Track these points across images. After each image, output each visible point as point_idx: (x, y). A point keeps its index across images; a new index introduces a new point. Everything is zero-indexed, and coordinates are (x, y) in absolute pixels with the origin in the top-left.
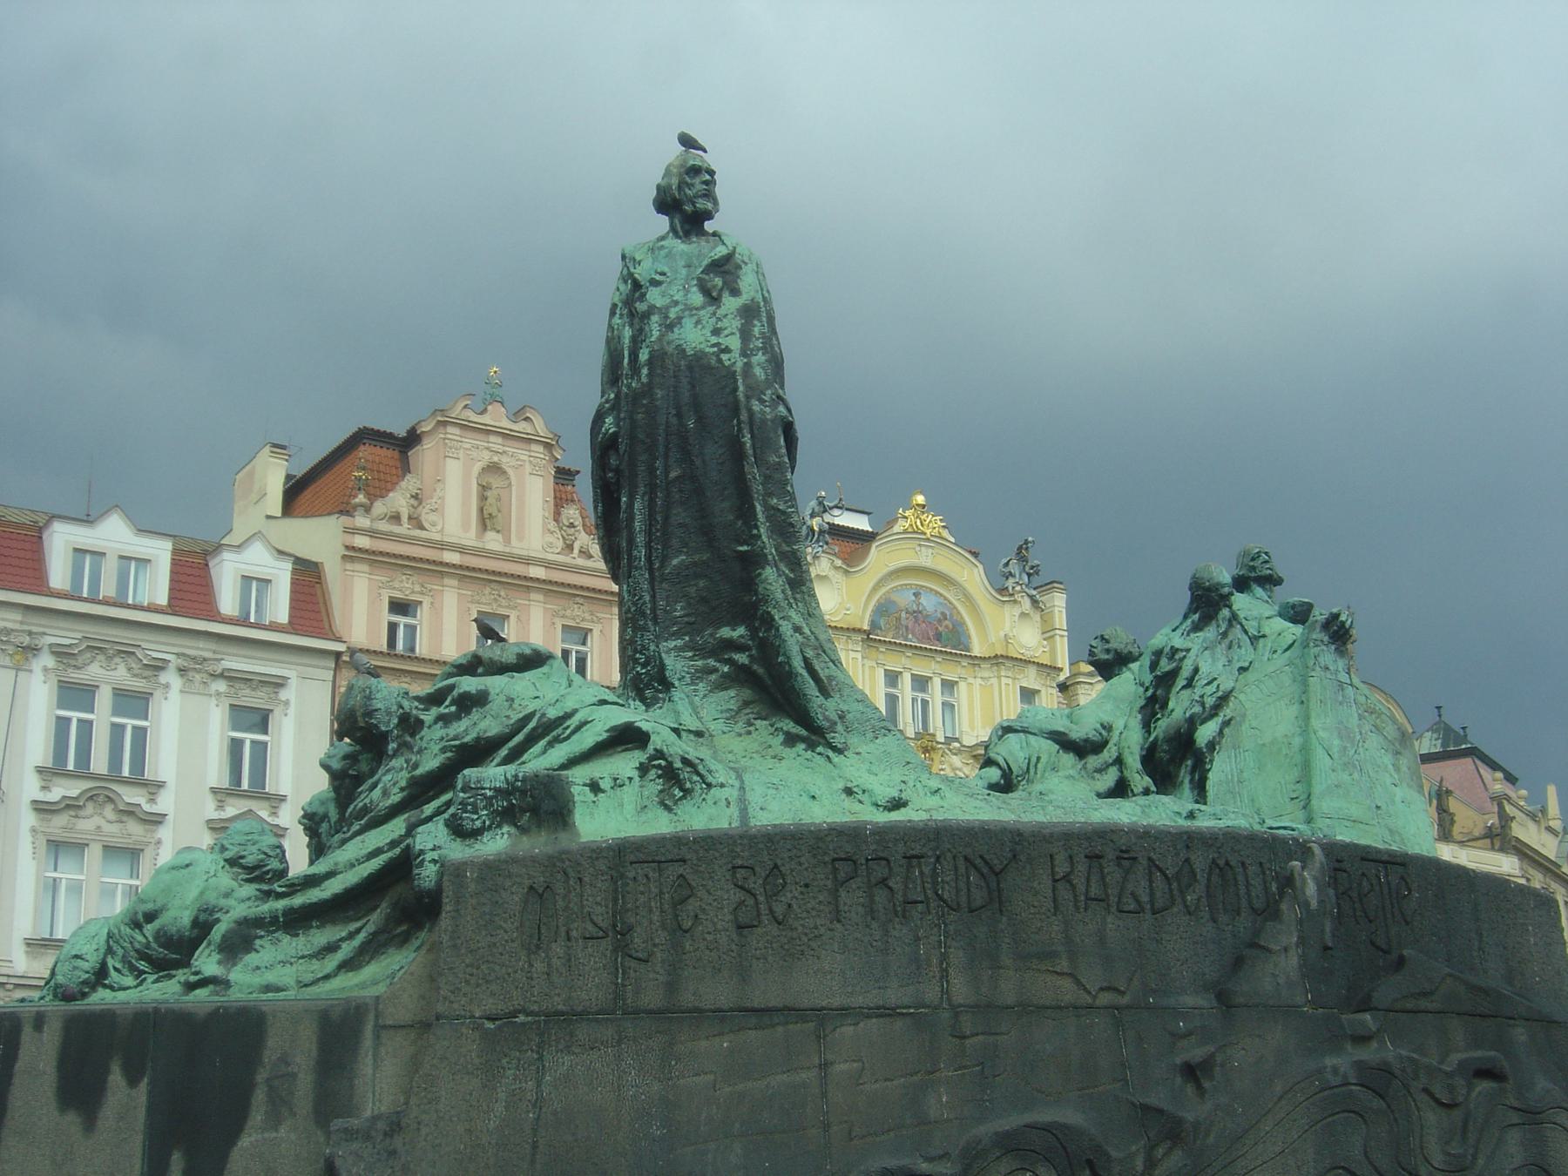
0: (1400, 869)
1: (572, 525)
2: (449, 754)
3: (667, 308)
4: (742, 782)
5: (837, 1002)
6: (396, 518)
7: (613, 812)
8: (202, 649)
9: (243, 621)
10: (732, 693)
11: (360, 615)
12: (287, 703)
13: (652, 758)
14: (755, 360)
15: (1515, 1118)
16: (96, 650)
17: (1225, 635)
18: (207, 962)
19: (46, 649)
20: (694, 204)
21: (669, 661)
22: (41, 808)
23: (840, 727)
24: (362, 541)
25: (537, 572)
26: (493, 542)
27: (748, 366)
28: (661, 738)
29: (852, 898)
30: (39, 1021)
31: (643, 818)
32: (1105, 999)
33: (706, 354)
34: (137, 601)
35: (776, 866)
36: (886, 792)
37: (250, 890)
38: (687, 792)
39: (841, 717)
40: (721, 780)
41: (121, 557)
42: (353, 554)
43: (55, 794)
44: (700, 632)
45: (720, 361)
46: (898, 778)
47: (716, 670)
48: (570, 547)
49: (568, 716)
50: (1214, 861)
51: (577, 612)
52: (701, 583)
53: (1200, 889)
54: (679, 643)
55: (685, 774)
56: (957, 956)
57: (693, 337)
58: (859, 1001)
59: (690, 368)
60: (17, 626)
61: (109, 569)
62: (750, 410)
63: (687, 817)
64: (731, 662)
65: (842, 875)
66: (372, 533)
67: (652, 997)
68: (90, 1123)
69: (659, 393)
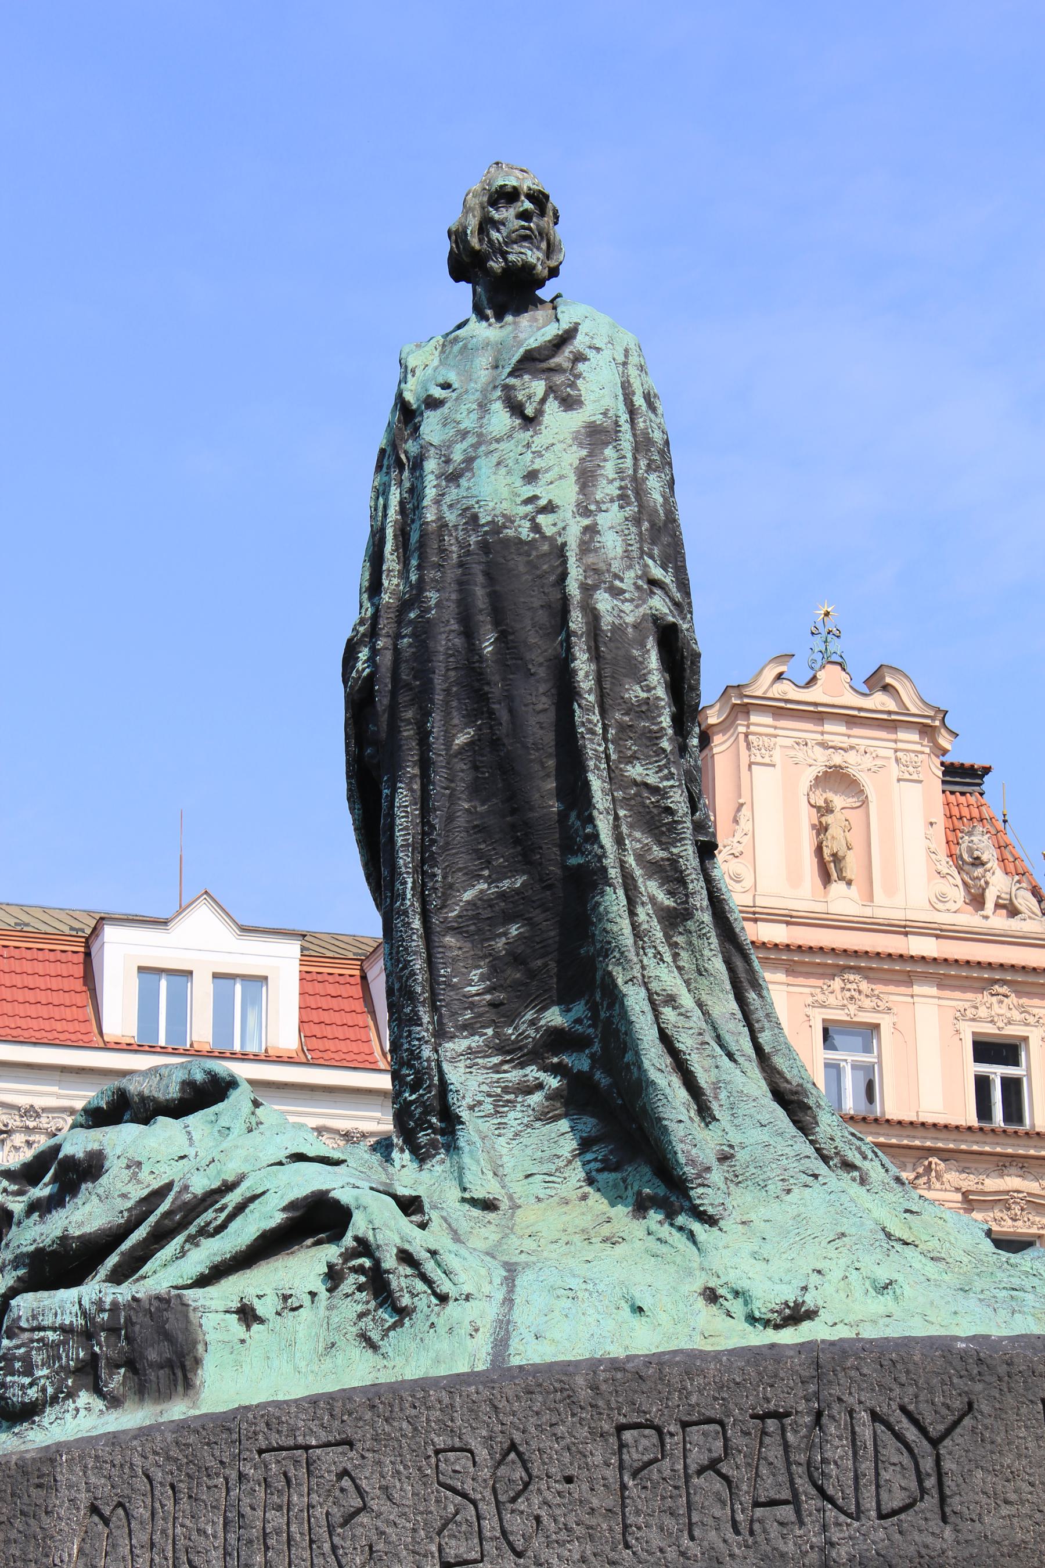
1: (978, 862)
2: (21, 1272)
3: (449, 445)
4: (511, 1290)
7: (271, 1351)
10: (564, 1125)
13: (349, 1255)
14: (604, 520)
20: (504, 254)
21: (455, 1075)
23: (716, 1176)
26: (842, 900)
28: (378, 1221)
31: (328, 1364)
33: (509, 520)
34: (252, 1048)
35: (513, 1447)
36: (771, 1292)
38: (403, 1313)
39: (724, 1158)
40: (466, 1289)
41: (216, 976)
44: (511, 1018)
45: (536, 528)
46: (806, 1266)
47: (540, 1086)
48: (977, 901)
49: (228, 1187)
51: (997, 1009)
52: (514, 930)
54: (476, 1041)
55: (401, 1279)
57: (495, 491)
59: (485, 547)
61: (202, 994)
62: (593, 617)
63: (399, 1361)
69: (432, 596)
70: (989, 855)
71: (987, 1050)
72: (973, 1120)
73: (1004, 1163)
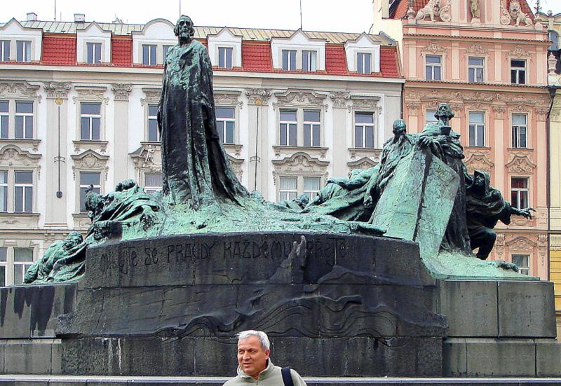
0: (342, 241)
3: (171, 72)
5: (167, 284)
6: (428, 18)
8: (341, 88)
9: (358, 74)
11: (412, 65)
12: (380, 108)
15: (363, 315)
16: (294, 94)
17: (400, 145)
18: (51, 275)
19: (273, 95)
22: (275, 163)
23: (198, 203)
24: (412, 31)
25: (498, 35)
26: (476, 23)
27: (191, 90)
28: (147, 211)
29: (173, 256)
30: (11, 289)
32: (235, 282)
36: (199, 223)
37: (67, 252)
42: (407, 38)
43: (282, 157)
49: (129, 203)
50: (274, 242)
53: (269, 250)
56: (197, 271)
58: (173, 284)
60: (260, 87)
61: (299, 56)
64: (185, 181)
65: (170, 250)
66: (417, 26)
67: (127, 283)
68: (20, 317)
70: (519, 9)
71: (514, 63)
72: (510, 84)
73: (517, 94)
